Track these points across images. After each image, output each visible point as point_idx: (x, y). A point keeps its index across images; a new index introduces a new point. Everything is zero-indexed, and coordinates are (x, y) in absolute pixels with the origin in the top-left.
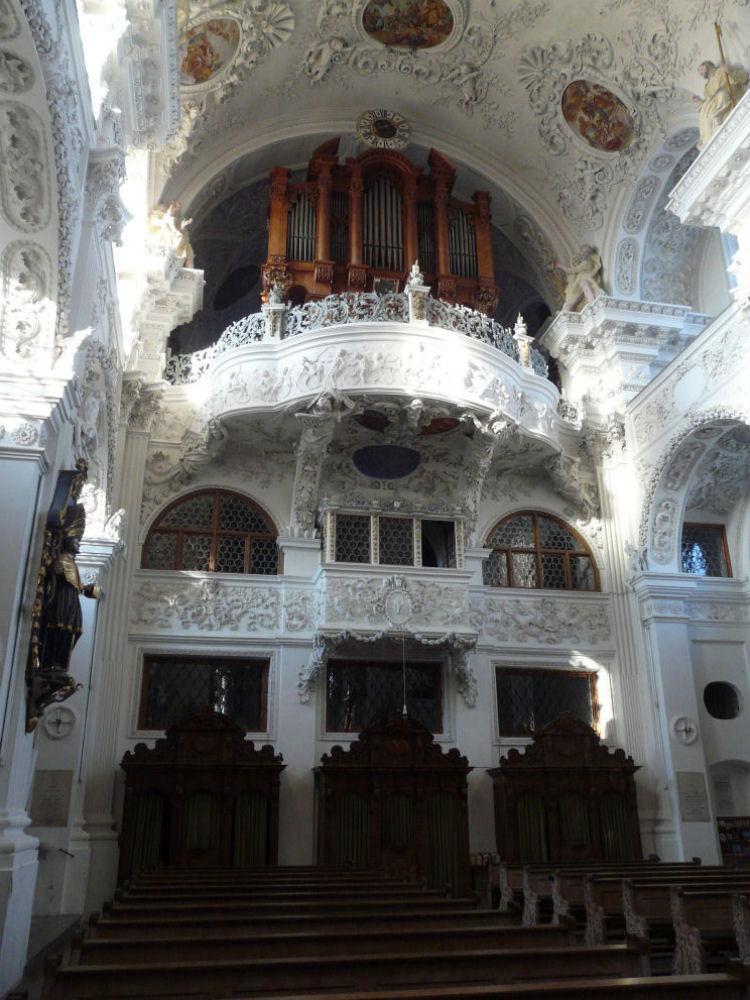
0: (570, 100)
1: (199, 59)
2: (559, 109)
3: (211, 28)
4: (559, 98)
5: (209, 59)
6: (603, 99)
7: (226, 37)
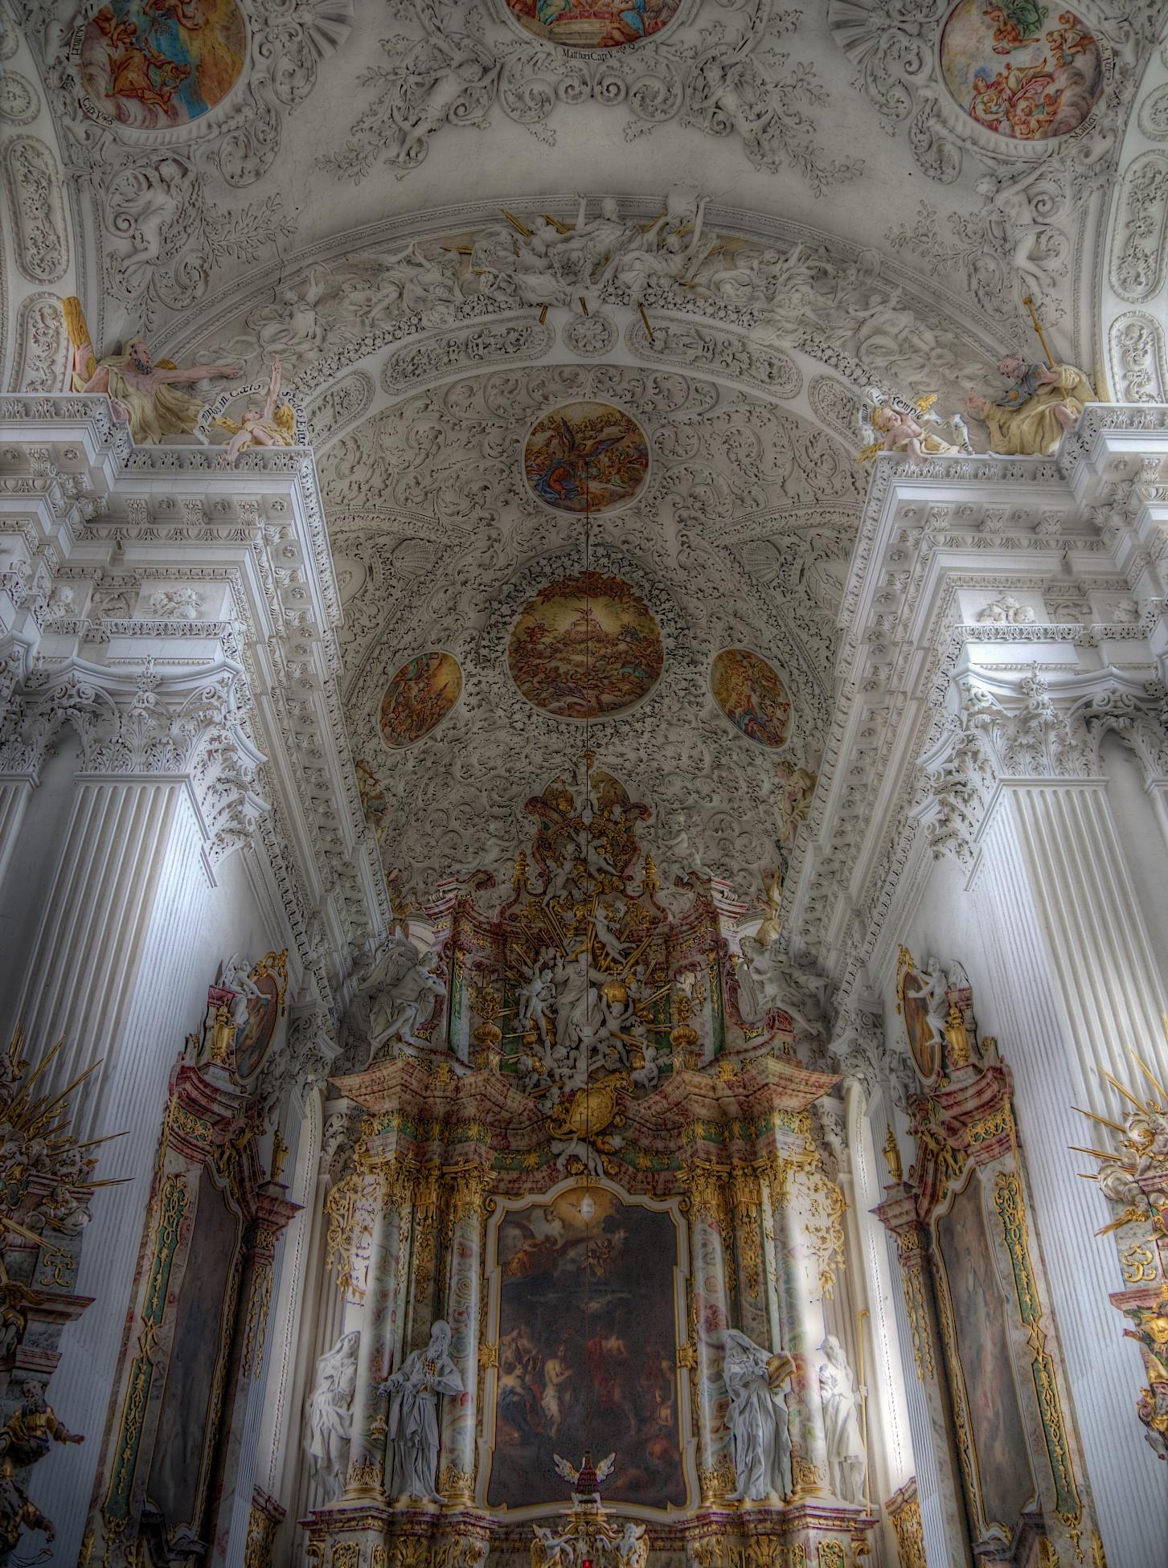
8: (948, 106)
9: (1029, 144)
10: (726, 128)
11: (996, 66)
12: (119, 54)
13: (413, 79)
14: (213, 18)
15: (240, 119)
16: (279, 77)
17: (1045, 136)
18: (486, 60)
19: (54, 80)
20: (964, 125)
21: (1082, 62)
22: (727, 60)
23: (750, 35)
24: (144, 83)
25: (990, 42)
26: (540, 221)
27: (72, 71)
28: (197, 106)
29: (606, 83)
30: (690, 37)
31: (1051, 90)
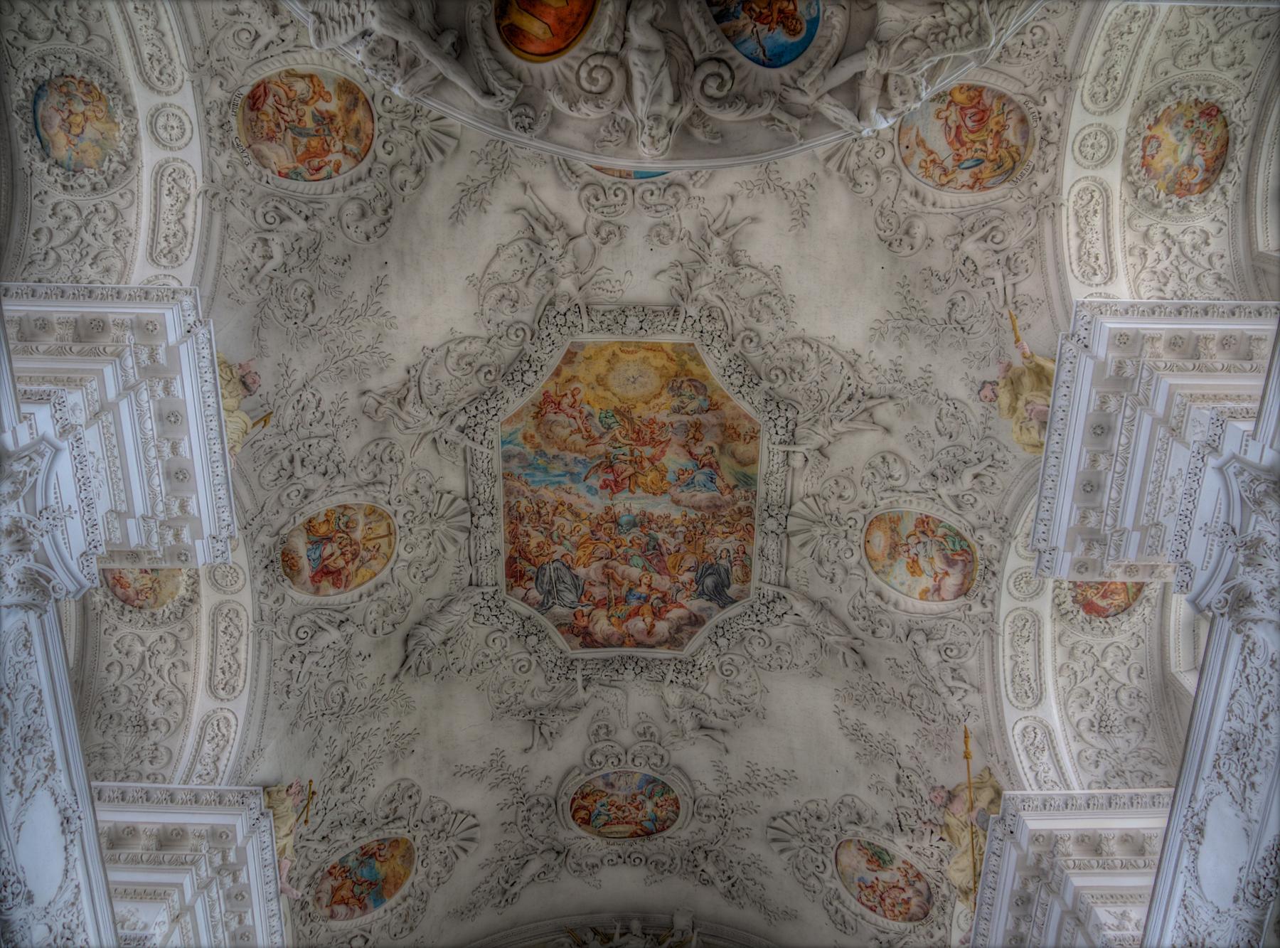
0: (360, 114)
1: (970, 124)
2: (366, 90)
3: (945, 172)
4: (378, 107)
5: (953, 115)
7: (921, 143)
8: (845, 895)
9: (896, 924)
10: (708, 882)
11: (870, 877)
12: (336, 884)
13: (513, 862)
14: (396, 853)
15: (405, 905)
16: (432, 874)
17: (904, 920)
18: (559, 848)
19: (298, 907)
20: (856, 907)
21: (919, 885)
22: (707, 848)
23: (720, 837)
24: (350, 895)
25: (864, 865)
26: (590, 935)
27: (309, 899)
28: (379, 900)
29: (633, 857)
30: (685, 834)
31: (904, 896)
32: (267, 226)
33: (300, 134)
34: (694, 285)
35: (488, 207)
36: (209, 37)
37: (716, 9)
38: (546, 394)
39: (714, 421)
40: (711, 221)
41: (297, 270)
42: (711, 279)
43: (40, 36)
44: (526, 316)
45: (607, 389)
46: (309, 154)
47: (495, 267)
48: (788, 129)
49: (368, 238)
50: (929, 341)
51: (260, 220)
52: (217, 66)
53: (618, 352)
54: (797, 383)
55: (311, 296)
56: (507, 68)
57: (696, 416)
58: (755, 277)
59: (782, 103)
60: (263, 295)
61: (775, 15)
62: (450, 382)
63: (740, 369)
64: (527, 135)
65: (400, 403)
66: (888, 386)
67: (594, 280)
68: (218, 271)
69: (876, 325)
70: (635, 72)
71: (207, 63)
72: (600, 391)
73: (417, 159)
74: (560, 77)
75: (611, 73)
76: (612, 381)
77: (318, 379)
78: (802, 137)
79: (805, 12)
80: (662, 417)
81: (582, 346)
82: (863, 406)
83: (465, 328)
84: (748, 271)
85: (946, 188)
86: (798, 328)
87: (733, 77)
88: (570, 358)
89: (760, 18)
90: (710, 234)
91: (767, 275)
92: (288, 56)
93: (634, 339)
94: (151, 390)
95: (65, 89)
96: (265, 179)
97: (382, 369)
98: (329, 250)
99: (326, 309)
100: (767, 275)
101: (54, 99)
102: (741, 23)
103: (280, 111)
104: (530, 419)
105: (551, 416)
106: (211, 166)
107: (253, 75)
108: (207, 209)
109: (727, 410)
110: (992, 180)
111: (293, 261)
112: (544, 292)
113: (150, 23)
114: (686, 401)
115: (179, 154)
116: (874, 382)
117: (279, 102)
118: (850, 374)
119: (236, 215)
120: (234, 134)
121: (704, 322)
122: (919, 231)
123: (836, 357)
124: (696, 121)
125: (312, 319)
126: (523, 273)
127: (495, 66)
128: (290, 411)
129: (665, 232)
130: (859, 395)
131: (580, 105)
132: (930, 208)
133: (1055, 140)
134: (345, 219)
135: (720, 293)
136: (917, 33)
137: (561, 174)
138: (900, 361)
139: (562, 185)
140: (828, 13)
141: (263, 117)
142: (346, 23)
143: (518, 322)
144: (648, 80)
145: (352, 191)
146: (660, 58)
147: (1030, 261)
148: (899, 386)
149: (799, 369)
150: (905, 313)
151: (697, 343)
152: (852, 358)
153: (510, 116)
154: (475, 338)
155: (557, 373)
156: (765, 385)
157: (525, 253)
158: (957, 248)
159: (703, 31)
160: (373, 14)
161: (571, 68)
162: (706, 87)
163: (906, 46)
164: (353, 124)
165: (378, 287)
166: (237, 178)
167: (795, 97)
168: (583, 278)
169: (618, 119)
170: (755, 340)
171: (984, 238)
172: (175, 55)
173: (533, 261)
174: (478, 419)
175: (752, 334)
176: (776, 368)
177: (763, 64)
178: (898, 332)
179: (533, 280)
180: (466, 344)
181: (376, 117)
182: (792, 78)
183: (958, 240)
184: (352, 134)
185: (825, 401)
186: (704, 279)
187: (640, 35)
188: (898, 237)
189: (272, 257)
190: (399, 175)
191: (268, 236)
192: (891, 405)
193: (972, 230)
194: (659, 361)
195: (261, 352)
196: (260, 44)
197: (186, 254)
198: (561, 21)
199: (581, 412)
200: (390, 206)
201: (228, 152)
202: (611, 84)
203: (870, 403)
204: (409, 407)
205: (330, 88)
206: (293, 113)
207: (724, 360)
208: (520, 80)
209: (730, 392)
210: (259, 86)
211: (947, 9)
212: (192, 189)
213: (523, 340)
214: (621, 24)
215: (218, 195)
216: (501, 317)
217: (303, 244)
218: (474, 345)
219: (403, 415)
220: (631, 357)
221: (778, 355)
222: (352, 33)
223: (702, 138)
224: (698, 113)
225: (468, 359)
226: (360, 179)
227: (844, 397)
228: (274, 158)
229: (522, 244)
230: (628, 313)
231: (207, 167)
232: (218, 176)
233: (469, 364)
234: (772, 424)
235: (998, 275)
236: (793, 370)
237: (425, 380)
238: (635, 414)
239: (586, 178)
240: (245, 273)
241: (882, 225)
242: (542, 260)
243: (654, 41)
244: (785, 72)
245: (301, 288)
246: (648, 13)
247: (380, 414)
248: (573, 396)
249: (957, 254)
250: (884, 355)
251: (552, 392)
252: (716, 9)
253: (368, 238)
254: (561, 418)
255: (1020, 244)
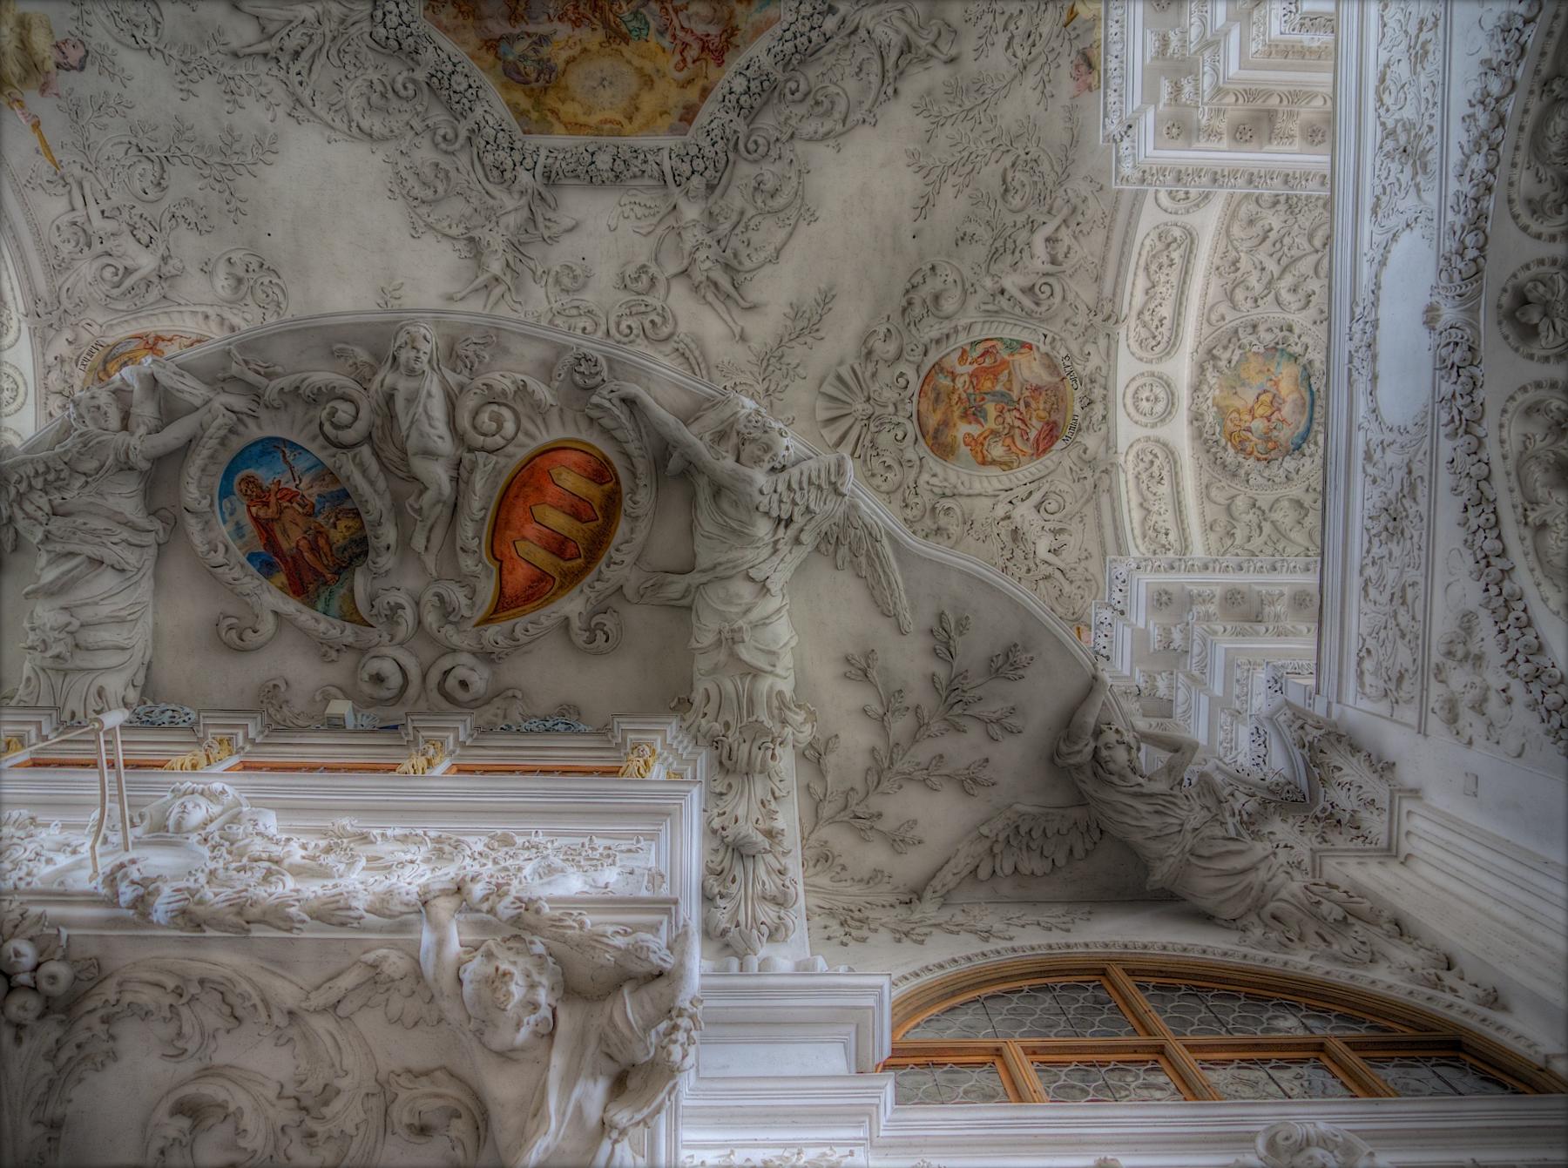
0: (932, 421)
2: (923, 449)
4: (912, 428)
6: (985, 370)
32: (1051, 280)
33: (1003, 395)
34: (526, 213)
35: (788, 310)
36: (1093, 503)
37: (348, 505)
38: (720, 63)
39: (491, 24)
40: (507, 296)
41: (1019, 225)
42: (503, 220)
43: (1285, 504)
44: (745, 171)
45: (640, 71)
46: (994, 372)
47: (782, 234)
48: (246, 362)
49: (933, 268)
50: (189, 134)
51: (1057, 289)
52: (1088, 473)
53: (625, 122)
54: (375, 77)
55: (1006, 190)
56: (607, 433)
57: (517, 31)
58: (445, 224)
59: (256, 394)
60: (1061, 191)
61: (273, 500)
62: (843, 78)
63: (456, 98)
64: (583, 350)
65: (907, 47)
66: (243, 72)
67: (658, 217)
68: (1113, 220)
69: (269, 157)
70: (441, 427)
71: (1097, 475)
72: (648, 67)
73: (870, 368)
74: (539, 422)
75: (475, 427)
76: (633, 82)
77: (1008, 78)
78: (229, 353)
79: (237, 504)
80: (563, 30)
81: (673, 130)
82: (275, 43)
83: (822, 153)
84: (454, 231)
85: (194, 337)
86: (380, 155)
87: (321, 425)
88: (689, 114)
89: (292, 496)
90: (508, 279)
91: (429, 226)
92: (1008, 486)
93: (604, 140)
94: (1184, 43)
95: (1270, 445)
96: (1048, 340)
97: (929, 94)
98: (979, 252)
99: (989, 176)
100: (429, 226)
101: (1285, 435)
102: (315, 490)
103: (1023, 421)
104: (742, 26)
105: (714, 30)
106: (1108, 355)
107: (1048, 463)
108: (1117, 300)
109: (473, 39)
110: (131, 347)
111: (1022, 236)
112: (721, 203)
113: (1154, 518)
114: (531, 53)
115: (1146, 368)
116: (264, 77)
117: (1024, 433)
118: (299, 89)
119: (1087, 295)
120: (1078, 394)
121: (509, 162)
122: (222, 283)
123: (323, 114)
124: (367, 371)
125: (1007, 161)
126: (747, 228)
127: (618, 434)
128: (1045, 30)
129: (566, 281)
130: (285, 59)
131: (513, 388)
132: (210, 311)
133: (52, 397)
134: (958, 292)
135: (491, 202)
136: (83, 479)
137: (697, 353)
138: (228, 107)
139: (698, 340)
140: (206, 502)
141: (1043, 414)
142: (800, 483)
143: (755, 161)
144: (424, 419)
145: (946, 327)
146: (412, 445)
147: (56, 241)
148: (226, 71)
149: (375, 98)
150: (229, 174)
151: (518, 133)
152: (301, 113)
153: (605, 374)
154: (810, 140)
155: (705, 93)
156: (421, 75)
157: (744, 251)
158: (165, 259)
159: (358, 478)
160: (761, 492)
161: (527, 434)
162: (353, 412)
163: (94, 464)
164: (942, 407)
165: (924, 206)
166: (1081, 340)
167: (239, 403)
168: (671, 221)
169: (466, 372)
170: (439, 139)
171: (128, 271)
172: (1132, 484)
173: (735, 242)
174: (808, 24)
175: (443, 146)
176: (407, 99)
177: (284, 441)
178: (237, 147)
179: (734, 218)
180: (822, 130)
181: (915, 418)
182: (246, 426)
183: (165, 270)
184: (943, 396)
185: (333, 52)
186: (512, 220)
187: (438, 474)
188: (251, 275)
189: (1048, 240)
190: (892, 348)
191: (1049, 268)
192: (235, 44)
193: (149, 284)
194: (569, 110)
195: (1071, 111)
196: (1036, 497)
197: (1148, 242)
198: (539, 489)
199: (674, 36)
200: (904, 310)
201: (1088, 371)
202: (476, 414)
203: (264, 46)
204: (896, 40)
205: (964, 450)
206: (1009, 420)
207: (479, 111)
208: (591, 420)
209: (469, 65)
210: (1044, 451)
211: (47, 508)
212: (1133, 325)
213: (748, 137)
214: (462, 485)
215: (1105, 316)
216: (777, 168)
217: (1009, 259)
218: (811, 129)
219: (904, 29)
220: (608, 115)
221: (406, 117)
222: (795, 472)
223: (358, 350)
224: (363, 382)
225: (821, 110)
226: (938, 342)
227: (306, 55)
228: (1036, 366)
229: (748, 264)
230: (611, 175)
231: (1112, 353)
232: (1102, 342)
233: (819, 104)
234: (406, 18)
235: (98, 222)
236: (383, 95)
237: (875, 80)
238: (600, 35)
239: (668, 348)
240: (1080, 218)
241: (277, 290)
242: (723, 244)
243: (420, 466)
244: (254, 432)
245: (1016, 202)
246: (428, 497)
247: (935, 29)
248: (684, 60)
249: (162, 250)
250: (253, 116)
251: (712, 64)
252: (348, 505)
253: (933, 268)
254: (700, 29)
255: (77, 264)
